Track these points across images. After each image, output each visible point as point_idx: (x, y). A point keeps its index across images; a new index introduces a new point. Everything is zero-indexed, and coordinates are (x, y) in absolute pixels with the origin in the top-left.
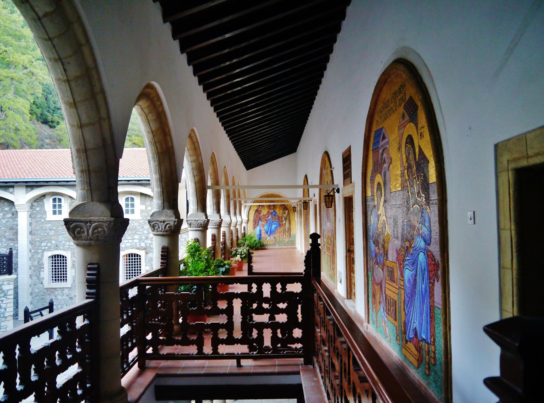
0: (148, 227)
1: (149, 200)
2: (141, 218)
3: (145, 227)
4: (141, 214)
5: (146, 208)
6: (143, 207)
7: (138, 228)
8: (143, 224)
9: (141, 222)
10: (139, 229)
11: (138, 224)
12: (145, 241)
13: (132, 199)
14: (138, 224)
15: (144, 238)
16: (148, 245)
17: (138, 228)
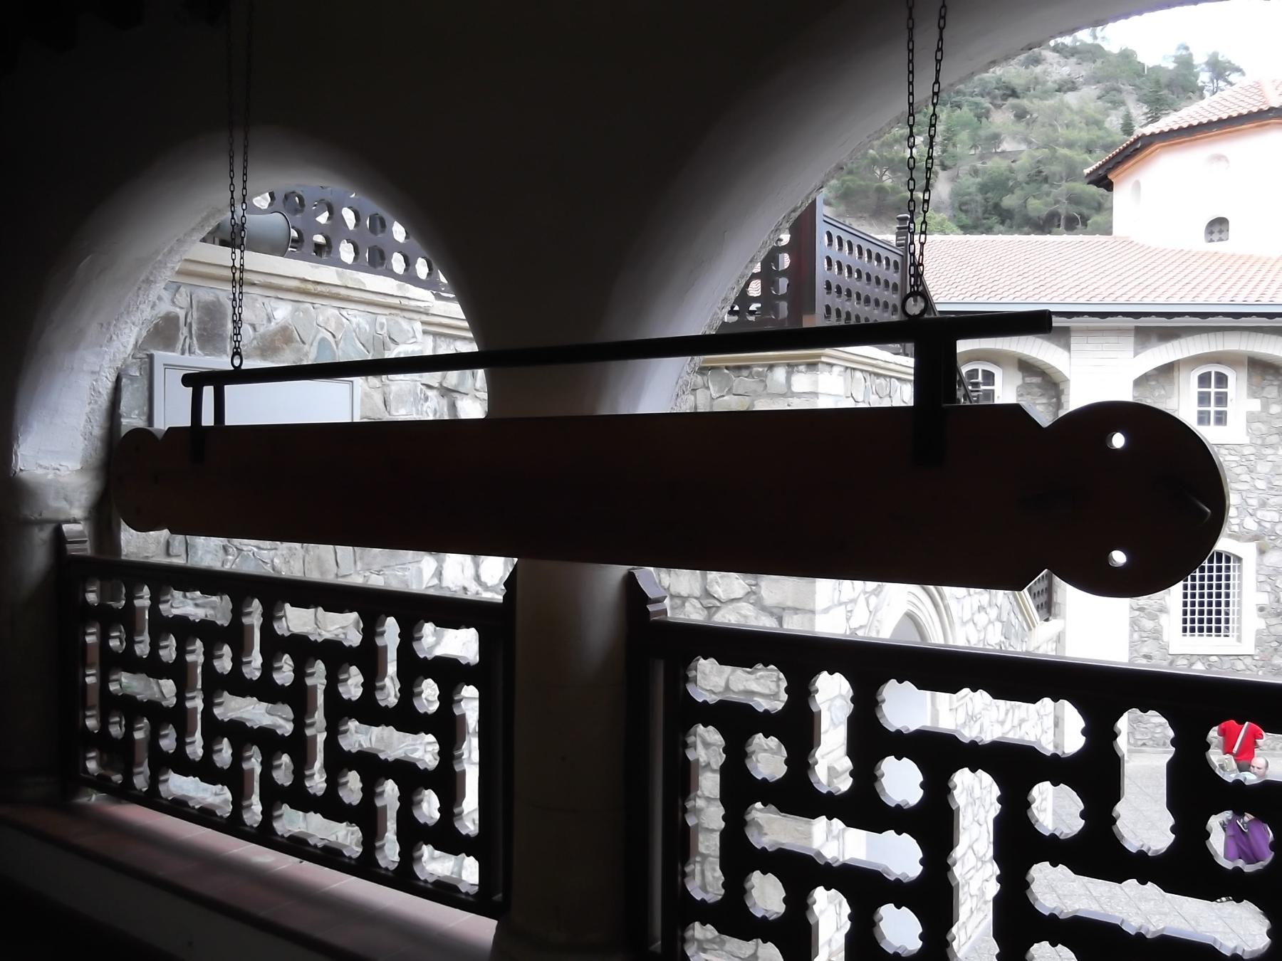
0: (1268, 470)
1: (1276, 383)
2: (1246, 440)
3: (1259, 468)
4: (1248, 427)
5: (1265, 407)
6: (1255, 405)
7: (1238, 470)
8: (1252, 458)
9: (1247, 451)
10: (1239, 475)
11: (1237, 458)
12: (1259, 514)
13: (1222, 379)
14: (1237, 458)
15: (1254, 502)
16: (1268, 525)
17: (1238, 470)
